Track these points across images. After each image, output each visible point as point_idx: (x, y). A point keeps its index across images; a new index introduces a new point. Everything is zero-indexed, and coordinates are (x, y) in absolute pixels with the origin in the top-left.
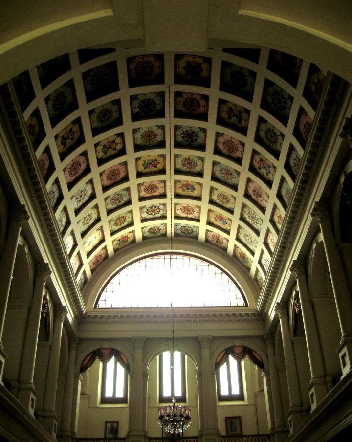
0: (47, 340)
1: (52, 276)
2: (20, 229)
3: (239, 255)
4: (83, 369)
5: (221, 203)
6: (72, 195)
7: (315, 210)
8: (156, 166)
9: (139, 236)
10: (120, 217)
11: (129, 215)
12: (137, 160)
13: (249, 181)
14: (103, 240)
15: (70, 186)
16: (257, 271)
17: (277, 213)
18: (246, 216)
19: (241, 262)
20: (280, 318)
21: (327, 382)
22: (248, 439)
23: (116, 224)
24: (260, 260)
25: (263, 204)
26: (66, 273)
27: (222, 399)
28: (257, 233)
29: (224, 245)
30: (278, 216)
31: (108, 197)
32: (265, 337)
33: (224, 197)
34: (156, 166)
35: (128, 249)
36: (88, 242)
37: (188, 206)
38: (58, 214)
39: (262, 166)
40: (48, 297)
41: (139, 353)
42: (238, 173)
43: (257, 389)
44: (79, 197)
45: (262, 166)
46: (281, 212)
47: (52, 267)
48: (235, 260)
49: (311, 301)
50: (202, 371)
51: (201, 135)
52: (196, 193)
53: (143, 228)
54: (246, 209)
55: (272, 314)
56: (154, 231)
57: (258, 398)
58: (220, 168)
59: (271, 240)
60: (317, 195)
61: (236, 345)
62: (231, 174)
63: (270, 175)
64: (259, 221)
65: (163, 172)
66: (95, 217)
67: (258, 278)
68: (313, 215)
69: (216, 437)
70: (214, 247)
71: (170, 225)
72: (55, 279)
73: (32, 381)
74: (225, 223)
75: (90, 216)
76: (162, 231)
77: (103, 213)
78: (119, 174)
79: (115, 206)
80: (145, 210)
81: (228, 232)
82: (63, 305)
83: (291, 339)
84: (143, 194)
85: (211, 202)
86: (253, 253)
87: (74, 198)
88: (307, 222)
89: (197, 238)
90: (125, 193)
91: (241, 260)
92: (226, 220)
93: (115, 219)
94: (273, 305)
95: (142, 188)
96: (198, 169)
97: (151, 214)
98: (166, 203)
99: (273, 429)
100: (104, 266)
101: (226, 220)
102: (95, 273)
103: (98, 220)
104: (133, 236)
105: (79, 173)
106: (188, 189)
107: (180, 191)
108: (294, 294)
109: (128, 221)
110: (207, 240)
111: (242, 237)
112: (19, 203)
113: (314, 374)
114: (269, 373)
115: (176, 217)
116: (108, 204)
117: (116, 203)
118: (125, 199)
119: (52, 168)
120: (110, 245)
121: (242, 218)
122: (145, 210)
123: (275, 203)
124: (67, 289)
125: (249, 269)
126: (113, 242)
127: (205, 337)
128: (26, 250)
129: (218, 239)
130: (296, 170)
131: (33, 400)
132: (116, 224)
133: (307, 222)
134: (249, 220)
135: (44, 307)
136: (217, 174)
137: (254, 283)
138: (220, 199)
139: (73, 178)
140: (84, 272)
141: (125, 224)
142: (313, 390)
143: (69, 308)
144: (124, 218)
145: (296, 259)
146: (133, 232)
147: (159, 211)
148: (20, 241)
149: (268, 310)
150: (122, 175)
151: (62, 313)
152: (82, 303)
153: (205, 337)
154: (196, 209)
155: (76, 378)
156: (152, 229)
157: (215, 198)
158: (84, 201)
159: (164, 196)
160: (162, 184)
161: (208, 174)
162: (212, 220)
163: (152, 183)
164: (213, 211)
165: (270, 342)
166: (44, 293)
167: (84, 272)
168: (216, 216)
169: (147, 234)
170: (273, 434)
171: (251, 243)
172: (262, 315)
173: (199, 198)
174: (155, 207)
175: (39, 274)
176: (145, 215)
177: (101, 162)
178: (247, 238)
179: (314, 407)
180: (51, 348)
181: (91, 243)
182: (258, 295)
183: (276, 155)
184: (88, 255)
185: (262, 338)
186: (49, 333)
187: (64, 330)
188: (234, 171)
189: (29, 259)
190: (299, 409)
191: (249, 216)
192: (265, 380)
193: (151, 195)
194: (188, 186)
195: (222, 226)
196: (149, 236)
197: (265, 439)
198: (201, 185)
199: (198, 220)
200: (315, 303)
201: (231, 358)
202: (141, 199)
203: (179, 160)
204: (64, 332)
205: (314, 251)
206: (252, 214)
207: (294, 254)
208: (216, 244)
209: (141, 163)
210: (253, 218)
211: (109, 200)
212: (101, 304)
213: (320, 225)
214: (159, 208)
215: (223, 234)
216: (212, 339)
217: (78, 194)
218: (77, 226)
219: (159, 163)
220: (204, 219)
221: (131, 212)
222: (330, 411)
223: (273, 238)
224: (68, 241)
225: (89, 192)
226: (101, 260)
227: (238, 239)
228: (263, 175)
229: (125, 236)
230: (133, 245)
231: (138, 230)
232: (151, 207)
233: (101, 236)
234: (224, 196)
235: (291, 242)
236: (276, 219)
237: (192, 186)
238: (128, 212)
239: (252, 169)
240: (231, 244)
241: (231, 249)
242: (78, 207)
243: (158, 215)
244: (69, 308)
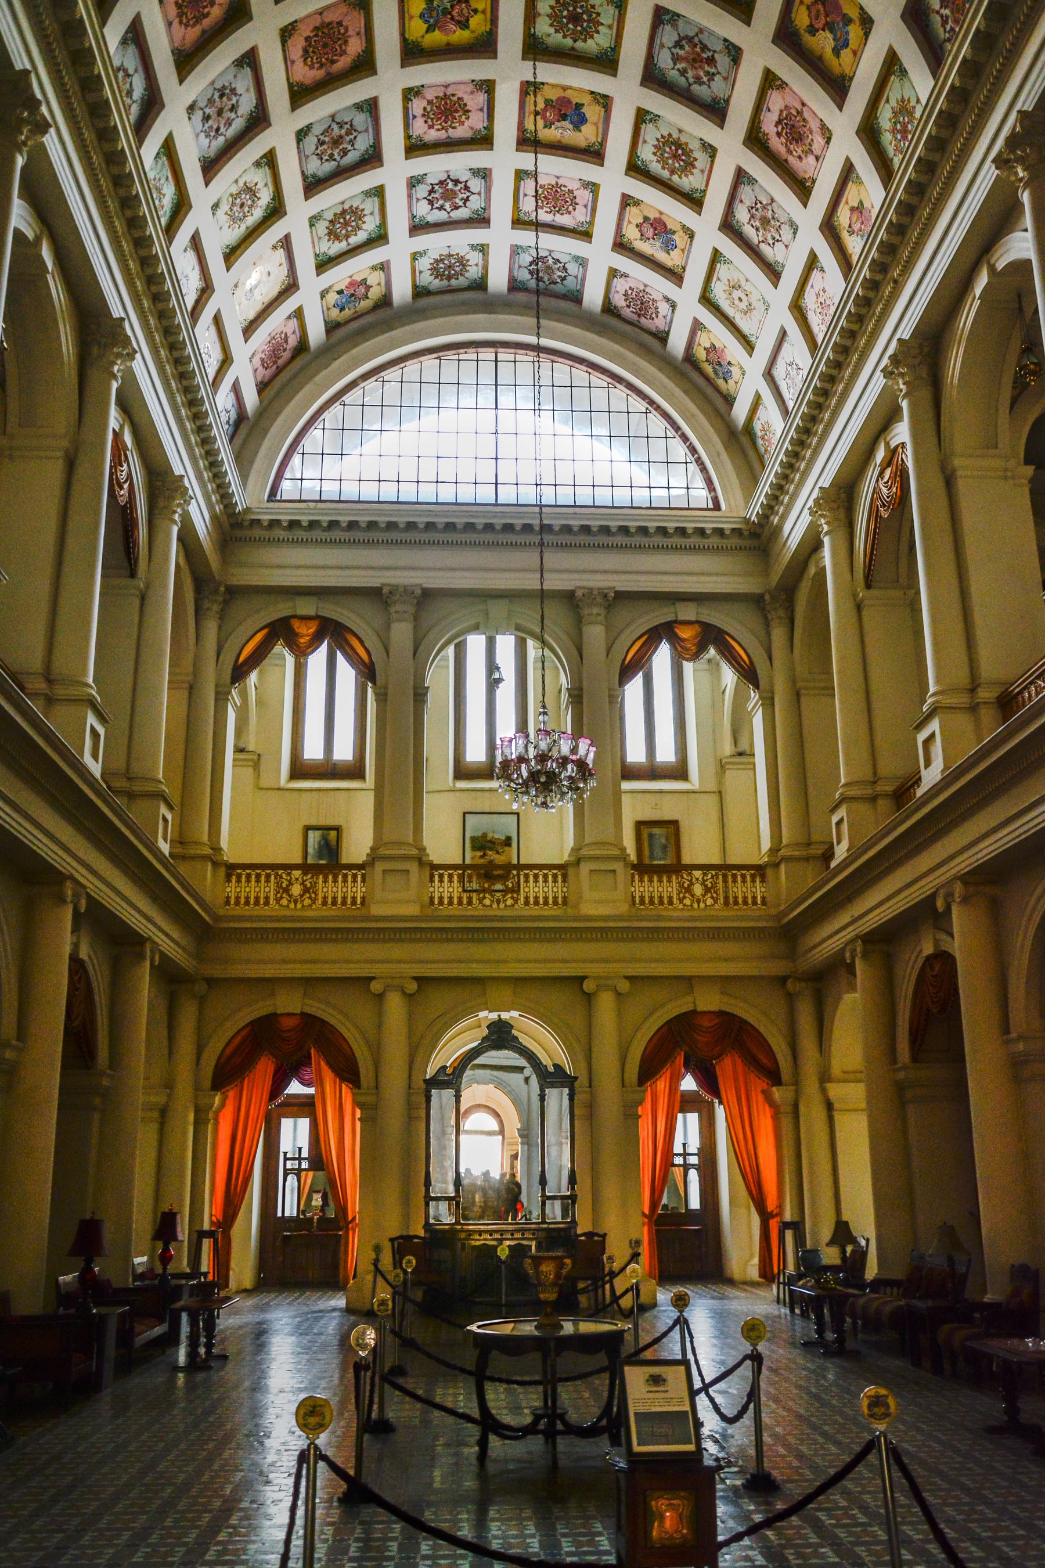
0: (133, 575)
2: (20, 161)
3: (701, 355)
4: (239, 673)
5: (665, 174)
6: (189, 102)
7: (1013, 142)
8: (464, 25)
10: (344, 212)
11: (371, 205)
14: (291, 287)
17: (852, 195)
19: (707, 379)
20: (827, 533)
21: (978, 703)
22: (705, 874)
23: (333, 235)
24: (768, 372)
25: (805, 166)
26: (181, 369)
27: (630, 773)
28: (773, 272)
29: (659, 323)
30: (853, 209)
31: (309, 127)
32: (767, 597)
34: (464, 25)
35: (367, 321)
36: (248, 287)
37: (560, 182)
39: (819, 25)
40: (128, 439)
41: (402, 632)
42: (735, 53)
43: (727, 748)
44: (214, 116)
45: (819, 25)
47: (135, 330)
48: (688, 368)
49: (943, 468)
50: (581, 689)
53: (415, 257)
54: (746, 193)
55: (795, 526)
56: (448, 267)
57: (727, 772)
58: (676, 38)
59: (818, 295)
61: (682, 617)
62: (711, 61)
63: (846, 54)
64: (786, 233)
67: (757, 426)
69: (618, 866)
70: (628, 328)
71: (499, 252)
73: (90, 680)
74: (669, 246)
75: (250, 191)
76: (473, 272)
78: (346, 42)
79: (329, 167)
80: (422, 191)
81: (676, 276)
82: (177, 473)
83: (855, 595)
85: (635, 168)
86: (749, 345)
87: (198, 115)
89: (576, 297)
91: (709, 369)
92: (674, 232)
93: (329, 216)
95: (418, 106)
97: (441, 208)
98: (490, 170)
99: (774, 850)
100: (292, 369)
101: (674, 232)
102: (270, 392)
104: (383, 283)
106: (563, 117)
111: (719, 292)
112: (12, 66)
113: (938, 680)
114: (772, 699)
116: (307, 157)
117: (331, 156)
121: (728, 226)
122: (422, 191)
123: (848, 159)
124: (188, 425)
125: (729, 400)
126: (323, 295)
127: (596, 592)
128: (46, 254)
129: (642, 304)
130: (945, 22)
131: (94, 733)
132: (333, 235)
134: (749, 231)
135: (115, 484)
137: (741, 443)
138: (662, 160)
139: (193, 33)
140: (236, 388)
141: (361, 237)
142: (934, 726)
143: (192, 484)
144: (357, 214)
145: (906, 336)
146: (383, 267)
147: (467, 199)
149: (784, 518)
151: (174, 499)
152: (232, 476)
153: (596, 592)
154: (584, 196)
155: (221, 698)
156: (442, 260)
157: (647, 154)
158: (230, 132)
160: (481, 98)
162: (631, 233)
163: (449, 91)
164: (637, 203)
165: (781, 613)
167: (236, 388)
168: (646, 219)
169: (426, 279)
170: (777, 865)
172: (757, 538)
173: (595, 154)
174: (456, 182)
175: (95, 350)
178: (737, 294)
179: (931, 775)
180: (143, 598)
181: (256, 292)
182: (755, 480)
184: (249, 330)
185: (756, 601)
186: (136, 560)
187: (182, 554)
188: (719, 46)
190: (869, 791)
191: (752, 216)
192: (758, 721)
193: (442, 135)
195: (661, 256)
196: (431, 287)
197: (753, 877)
198: (605, 102)
199: (585, 235)
200: (959, 473)
201: (662, 657)
202: (415, 148)
204: (182, 561)
205: (977, 303)
206: (764, 207)
208: (635, 317)
210: (765, 222)
212: (288, 488)
213: (1026, 197)
214: (467, 188)
215: (658, 285)
216: (615, 598)
217: (211, 101)
219: (476, 11)
221: (379, 192)
222: (977, 787)
223: (831, 286)
226: (286, 355)
227: (706, 299)
228: (821, 58)
229: (358, 278)
230: (381, 314)
232: (441, 182)
233: (284, 270)
234: (678, 144)
235: (895, 282)
237: (579, 106)
238: (368, 194)
242: (212, 153)
243: (463, 213)
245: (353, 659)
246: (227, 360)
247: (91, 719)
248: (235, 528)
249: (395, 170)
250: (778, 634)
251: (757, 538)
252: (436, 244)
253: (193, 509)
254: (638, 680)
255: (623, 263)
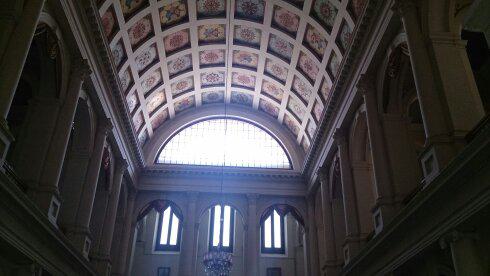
1: (114, 131)
9: (198, 99)
12: (200, 28)
13: (301, 54)
14: (165, 102)
15: (135, 47)
16: (303, 137)
17: (325, 84)
18: (297, 87)
23: (178, 88)
24: (305, 129)
25: (312, 76)
27: (265, 250)
28: (306, 103)
33: (278, 68)
38: (122, 73)
42: (292, 46)
43: (298, 244)
46: (329, 84)
47: (114, 121)
51: (260, 7)
52: (252, 64)
55: (314, 177)
60: (363, 68)
65: (223, 41)
66: (158, 79)
68: (359, 86)
71: (228, 91)
72: (117, 133)
76: (220, 98)
77: (166, 77)
81: (279, 102)
84: (204, 61)
85: (266, 73)
86: (300, 122)
88: (352, 93)
90: (187, 59)
94: (316, 169)
95: (203, 56)
96: (255, 40)
100: (167, 126)
103: (161, 83)
105: (143, 37)
107: (237, 61)
108: (335, 160)
109: (189, 86)
110: (260, 108)
111: (291, 107)
115: (233, 85)
118: (187, 65)
119: (116, 28)
120: (171, 106)
122: (204, 77)
125: (296, 136)
132: (178, 88)
133: (352, 93)
135: (103, 163)
136: (273, 46)
137: (300, 147)
141: (186, 88)
142: (347, 247)
143: (129, 161)
146: (194, 96)
148: (81, 94)
150: (185, 41)
155: (133, 225)
157: (269, 69)
159: (222, 64)
161: (264, 47)
162: (266, 89)
166: (105, 146)
171: (300, 112)
173: (254, 69)
176: (205, 82)
177: (164, 27)
183: (329, 29)
189: (91, 112)
194: (246, 57)
195: (275, 96)
199: (253, 89)
203: (239, 31)
207: (338, 123)
209: (203, 31)
211: (171, 65)
215: (275, 104)
218: (141, 86)
220: (258, 89)
221: (192, 77)
223: (320, 108)
224: (131, 100)
225: (153, 56)
227: (288, 108)
231: (198, 94)
236: (323, 90)
239: (305, 43)
240: (282, 112)
241: (281, 117)
244: (129, 161)
245: (178, 216)
246: (144, 123)
247: (87, 239)
248: (142, 172)
249: (197, 72)
250: (310, 208)
251: (304, 178)
252: (208, 90)
253: (129, 168)
254: (269, 219)
255: (263, 97)
